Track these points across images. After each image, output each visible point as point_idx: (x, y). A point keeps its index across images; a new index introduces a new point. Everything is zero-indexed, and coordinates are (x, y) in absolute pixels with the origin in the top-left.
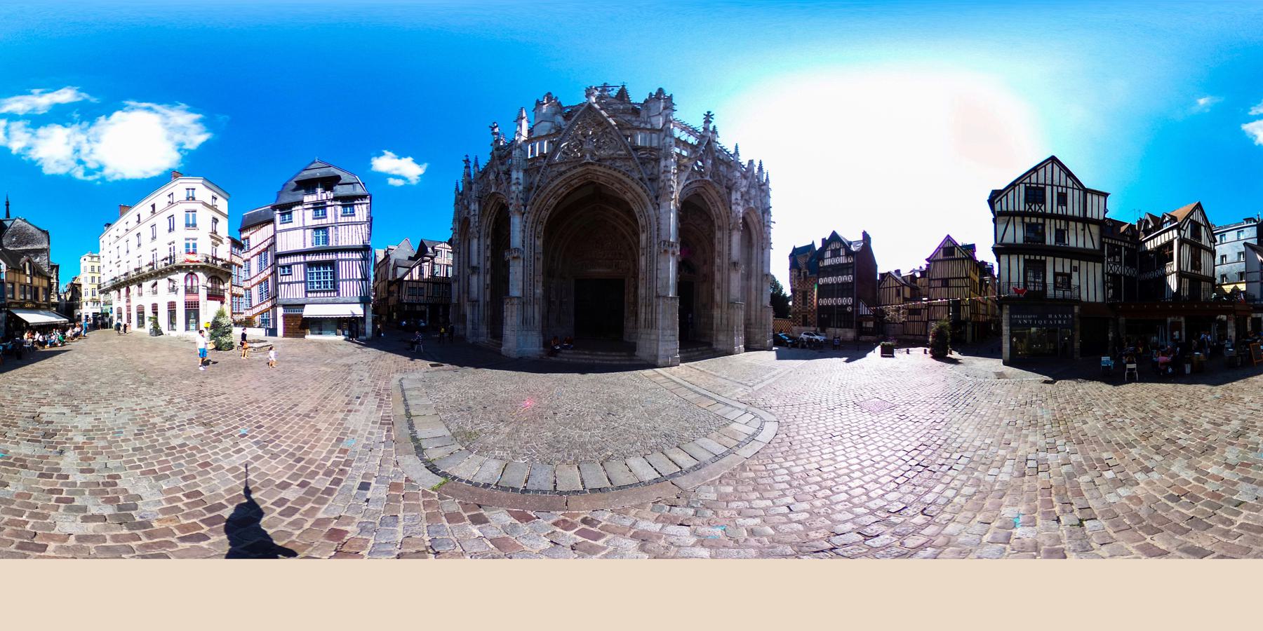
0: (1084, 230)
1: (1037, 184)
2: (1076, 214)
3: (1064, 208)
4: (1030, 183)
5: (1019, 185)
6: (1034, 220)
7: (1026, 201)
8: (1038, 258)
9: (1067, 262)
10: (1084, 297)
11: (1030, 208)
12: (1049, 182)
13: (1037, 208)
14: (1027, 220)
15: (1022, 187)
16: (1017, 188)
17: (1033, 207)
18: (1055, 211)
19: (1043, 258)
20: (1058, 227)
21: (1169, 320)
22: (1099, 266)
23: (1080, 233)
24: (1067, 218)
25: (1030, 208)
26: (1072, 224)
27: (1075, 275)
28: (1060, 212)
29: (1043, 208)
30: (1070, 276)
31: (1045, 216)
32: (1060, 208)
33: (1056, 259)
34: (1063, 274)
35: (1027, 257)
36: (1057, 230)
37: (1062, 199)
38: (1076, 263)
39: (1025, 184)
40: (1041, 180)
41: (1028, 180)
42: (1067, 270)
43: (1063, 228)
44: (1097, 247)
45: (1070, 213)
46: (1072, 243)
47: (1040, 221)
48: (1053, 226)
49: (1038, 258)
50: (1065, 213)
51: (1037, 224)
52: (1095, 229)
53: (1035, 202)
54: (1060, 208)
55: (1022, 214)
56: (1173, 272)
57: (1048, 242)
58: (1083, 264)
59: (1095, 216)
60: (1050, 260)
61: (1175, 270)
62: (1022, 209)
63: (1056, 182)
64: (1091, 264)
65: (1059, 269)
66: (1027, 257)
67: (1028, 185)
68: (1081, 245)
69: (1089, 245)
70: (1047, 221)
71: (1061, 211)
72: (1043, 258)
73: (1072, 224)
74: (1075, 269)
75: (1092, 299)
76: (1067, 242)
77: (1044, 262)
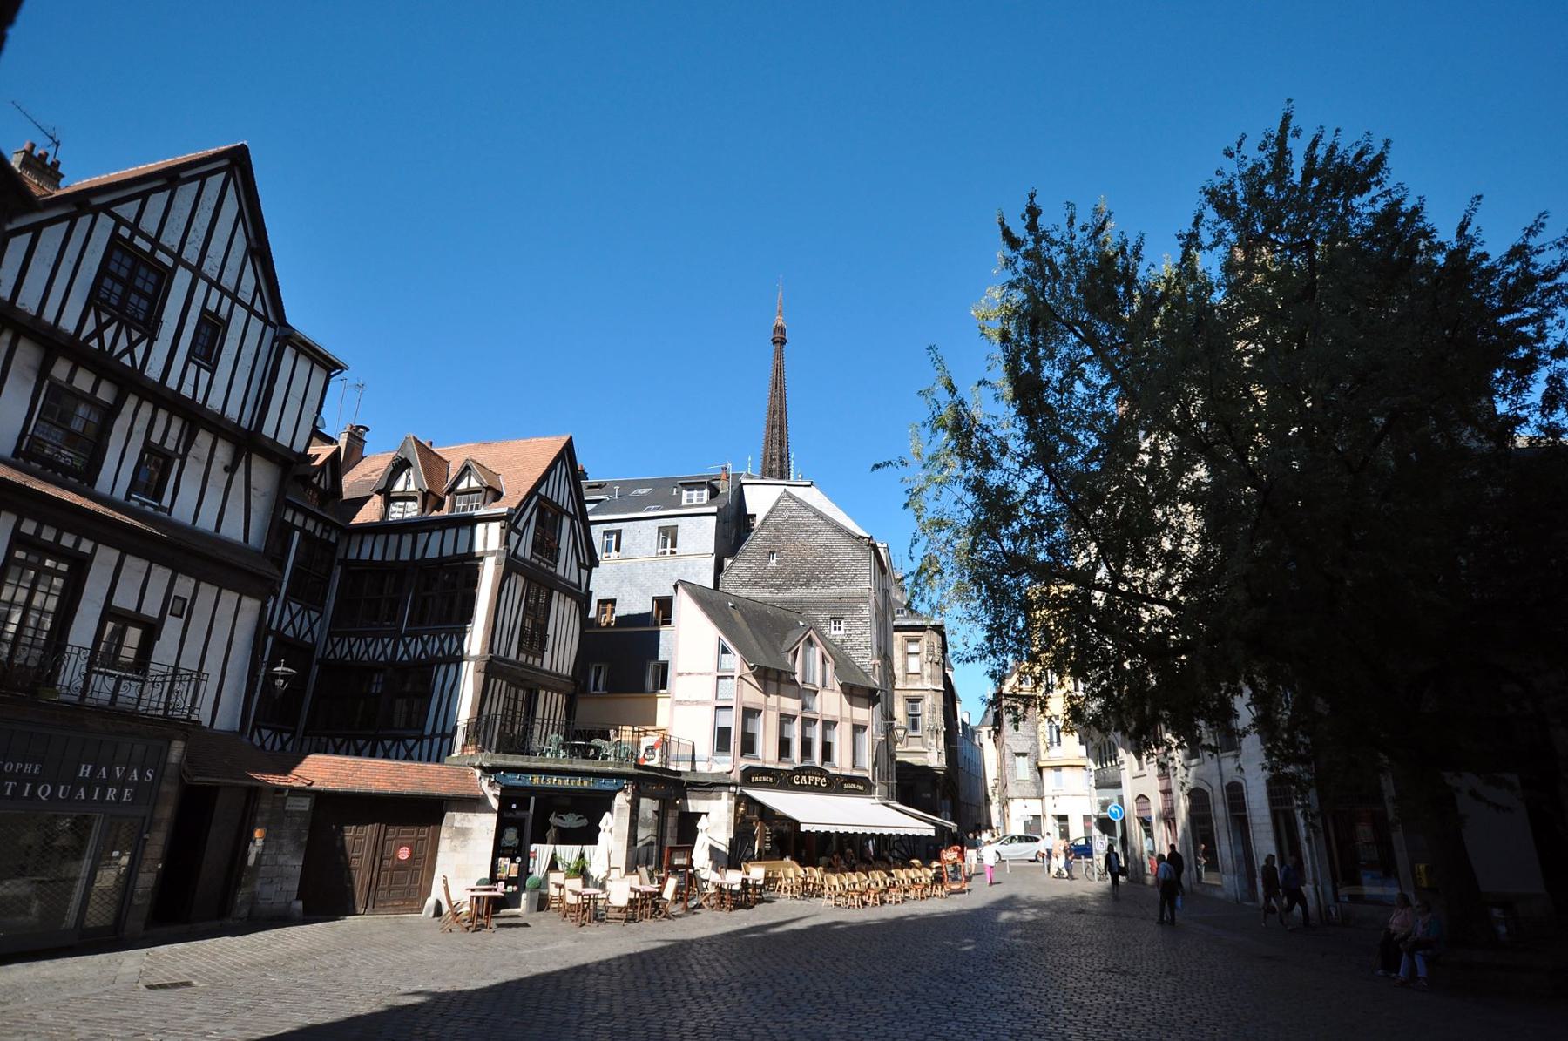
0: (231, 469)
1: (155, 242)
2: (232, 412)
3: (205, 375)
4: (135, 228)
5: (95, 213)
6: (84, 381)
7: (94, 301)
8: (68, 541)
9: (161, 576)
11: (98, 333)
12: (191, 254)
13: (122, 343)
14: (61, 370)
15: (105, 224)
16: (84, 222)
17: (109, 334)
18: (172, 383)
19: (86, 546)
20: (156, 438)
22: (251, 606)
23: (218, 477)
24: (194, 416)
25: (98, 333)
26: (204, 439)
27: (172, 627)
28: (187, 391)
29: (139, 351)
31: (131, 383)
32: (192, 368)
33: (129, 560)
34: (135, 618)
35: (29, 527)
36: (148, 446)
37: (207, 348)
38: (184, 586)
39: (120, 221)
40: (171, 238)
41: (128, 211)
42: (151, 608)
43: (170, 445)
46: (183, 512)
47: (106, 393)
48: (141, 426)
49: (68, 541)
51: (90, 399)
52: (263, 474)
53: (125, 320)
54: (192, 368)
55: (52, 343)
58: (207, 592)
60: (106, 557)
62: (69, 323)
63: (211, 267)
64: (230, 597)
65: (125, 599)
66: (29, 527)
67: (125, 232)
68: (207, 522)
69: (233, 529)
71: (186, 381)
72: (86, 546)
73: (204, 439)
76: (166, 502)
77: (80, 566)
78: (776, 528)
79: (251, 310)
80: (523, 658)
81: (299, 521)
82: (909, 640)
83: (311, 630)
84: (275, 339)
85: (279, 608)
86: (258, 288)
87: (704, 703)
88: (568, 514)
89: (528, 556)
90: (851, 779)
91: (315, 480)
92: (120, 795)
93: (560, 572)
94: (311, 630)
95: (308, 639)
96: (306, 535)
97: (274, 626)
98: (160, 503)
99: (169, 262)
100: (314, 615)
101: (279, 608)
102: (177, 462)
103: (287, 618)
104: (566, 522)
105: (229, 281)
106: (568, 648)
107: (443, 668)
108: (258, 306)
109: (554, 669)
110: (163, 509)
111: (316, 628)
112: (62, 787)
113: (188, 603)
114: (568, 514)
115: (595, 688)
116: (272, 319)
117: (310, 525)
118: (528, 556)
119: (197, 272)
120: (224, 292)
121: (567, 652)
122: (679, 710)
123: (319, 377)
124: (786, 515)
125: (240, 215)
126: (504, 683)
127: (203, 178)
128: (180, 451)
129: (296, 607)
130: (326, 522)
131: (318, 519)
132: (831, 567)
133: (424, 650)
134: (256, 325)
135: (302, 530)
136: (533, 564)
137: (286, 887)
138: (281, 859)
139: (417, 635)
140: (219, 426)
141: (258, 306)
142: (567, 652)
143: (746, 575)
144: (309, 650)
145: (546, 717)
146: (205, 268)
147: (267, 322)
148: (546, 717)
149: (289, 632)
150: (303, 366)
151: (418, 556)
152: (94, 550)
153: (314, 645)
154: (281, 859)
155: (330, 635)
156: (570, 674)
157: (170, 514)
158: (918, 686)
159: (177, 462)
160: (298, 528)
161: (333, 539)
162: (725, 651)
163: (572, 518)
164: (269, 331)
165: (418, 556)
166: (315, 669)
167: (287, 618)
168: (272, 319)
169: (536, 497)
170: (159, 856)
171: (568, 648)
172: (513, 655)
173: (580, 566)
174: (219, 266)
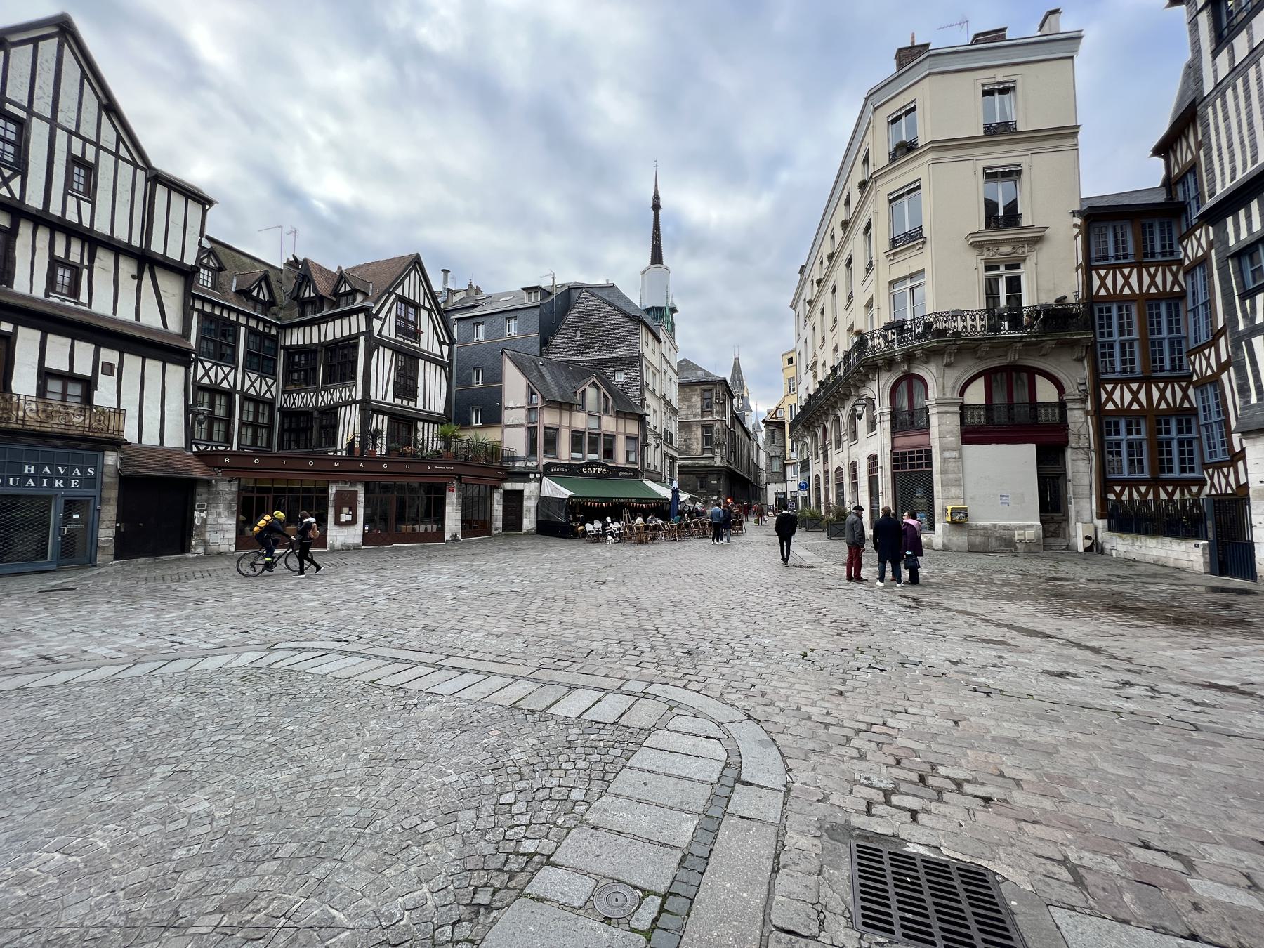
2: (121, 234)
10: (130, 434)
21: (333, 490)
28: (72, 216)
30: (89, 385)
32: (71, 202)
34: (68, 377)
38: (108, 355)
42: (83, 367)
44: (174, 326)
45: (102, 226)
46: (101, 305)
50: (86, 223)
54: (71, 202)
56: (355, 402)
57: (21, 284)
58: (132, 363)
59: (174, 254)
61: (359, 397)
69: (151, 318)
70: (25, 230)
74: (109, 369)
75: (151, 438)
76: (84, 297)
78: (579, 313)
79: (116, 154)
80: (398, 401)
81: (242, 320)
82: (704, 390)
83: (269, 390)
84: (147, 180)
85: (239, 376)
86: (119, 138)
87: (522, 425)
88: (426, 309)
89: (393, 336)
90: (624, 469)
91: (255, 293)
92: (67, 484)
93: (423, 346)
94: (269, 390)
95: (268, 395)
96: (251, 331)
97: (238, 388)
98: (78, 299)
99: (23, 115)
100: (270, 382)
101: (239, 376)
102: (85, 272)
103: (248, 383)
104: (424, 314)
105: (88, 130)
106: (438, 395)
107: (343, 408)
108: (123, 152)
109: (427, 409)
110: (84, 304)
111: (273, 389)
112: (11, 479)
113: (116, 366)
114: (426, 309)
115: (477, 422)
116: (140, 163)
117: (253, 323)
118: (393, 336)
119: (53, 122)
120: (85, 140)
121: (437, 398)
122: (507, 430)
123: (195, 210)
124: (585, 304)
125: (84, 76)
126: (386, 418)
127: (35, 41)
128: (86, 263)
129: (254, 376)
130: (265, 322)
131: (258, 319)
132: (615, 337)
133: (332, 399)
134: (126, 170)
135: (246, 326)
136: (396, 341)
137: (227, 536)
138: (221, 521)
139: (326, 390)
140: (119, 250)
141: (123, 152)
142: (437, 398)
143: (561, 346)
144: (271, 403)
145: (426, 435)
146: (61, 118)
147: (136, 166)
148: (426, 435)
149: (252, 391)
150: (178, 201)
151: (322, 340)
152: (15, 330)
153: (273, 399)
154: (221, 521)
155: (283, 393)
156: (442, 412)
157: (90, 306)
158: (710, 418)
159: (85, 272)
160: (243, 325)
161: (274, 332)
162: (533, 393)
163: (430, 311)
164: (141, 175)
165: (322, 340)
166: (278, 414)
167: (248, 383)
168: (140, 163)
169: (394, 296)
170: (114, 518)
171: (438, 395)
172: (390, 399)
173: (441, 343)
174: (75, 118)
